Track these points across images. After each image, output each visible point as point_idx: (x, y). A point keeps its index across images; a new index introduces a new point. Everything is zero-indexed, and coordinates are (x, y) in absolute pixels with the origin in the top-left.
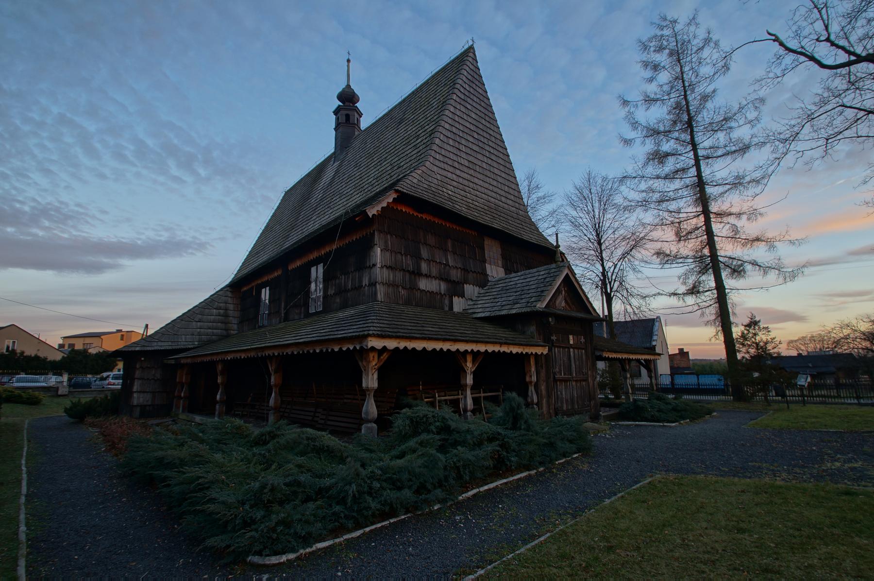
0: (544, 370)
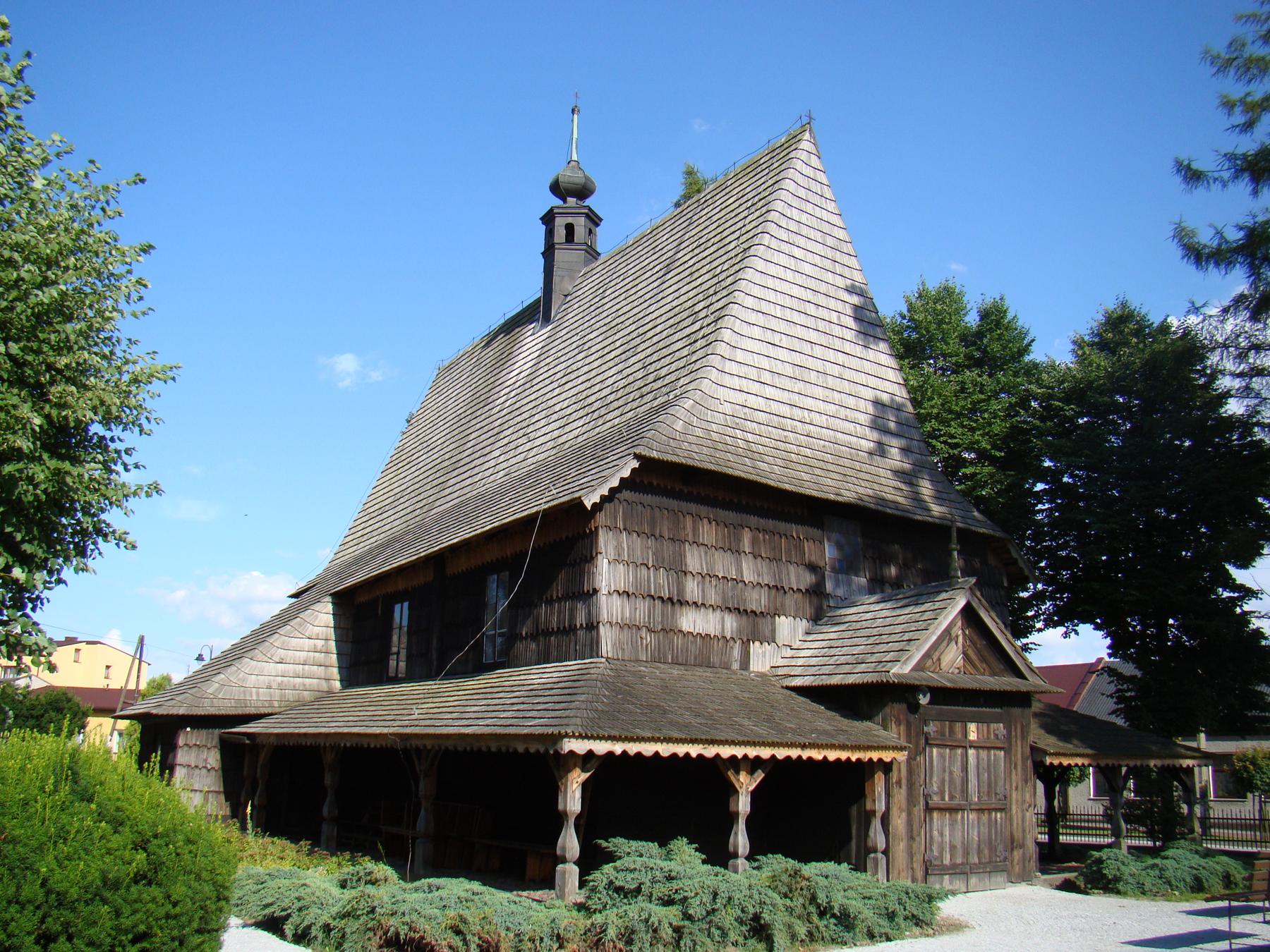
0: (904, 791)
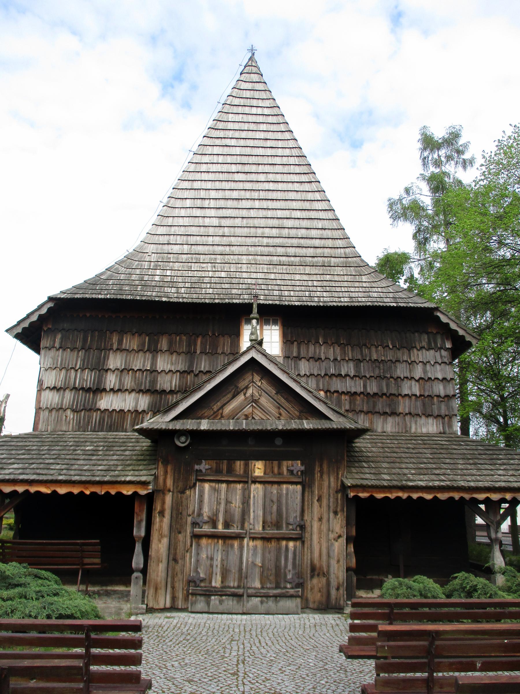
0: (167, 520)
